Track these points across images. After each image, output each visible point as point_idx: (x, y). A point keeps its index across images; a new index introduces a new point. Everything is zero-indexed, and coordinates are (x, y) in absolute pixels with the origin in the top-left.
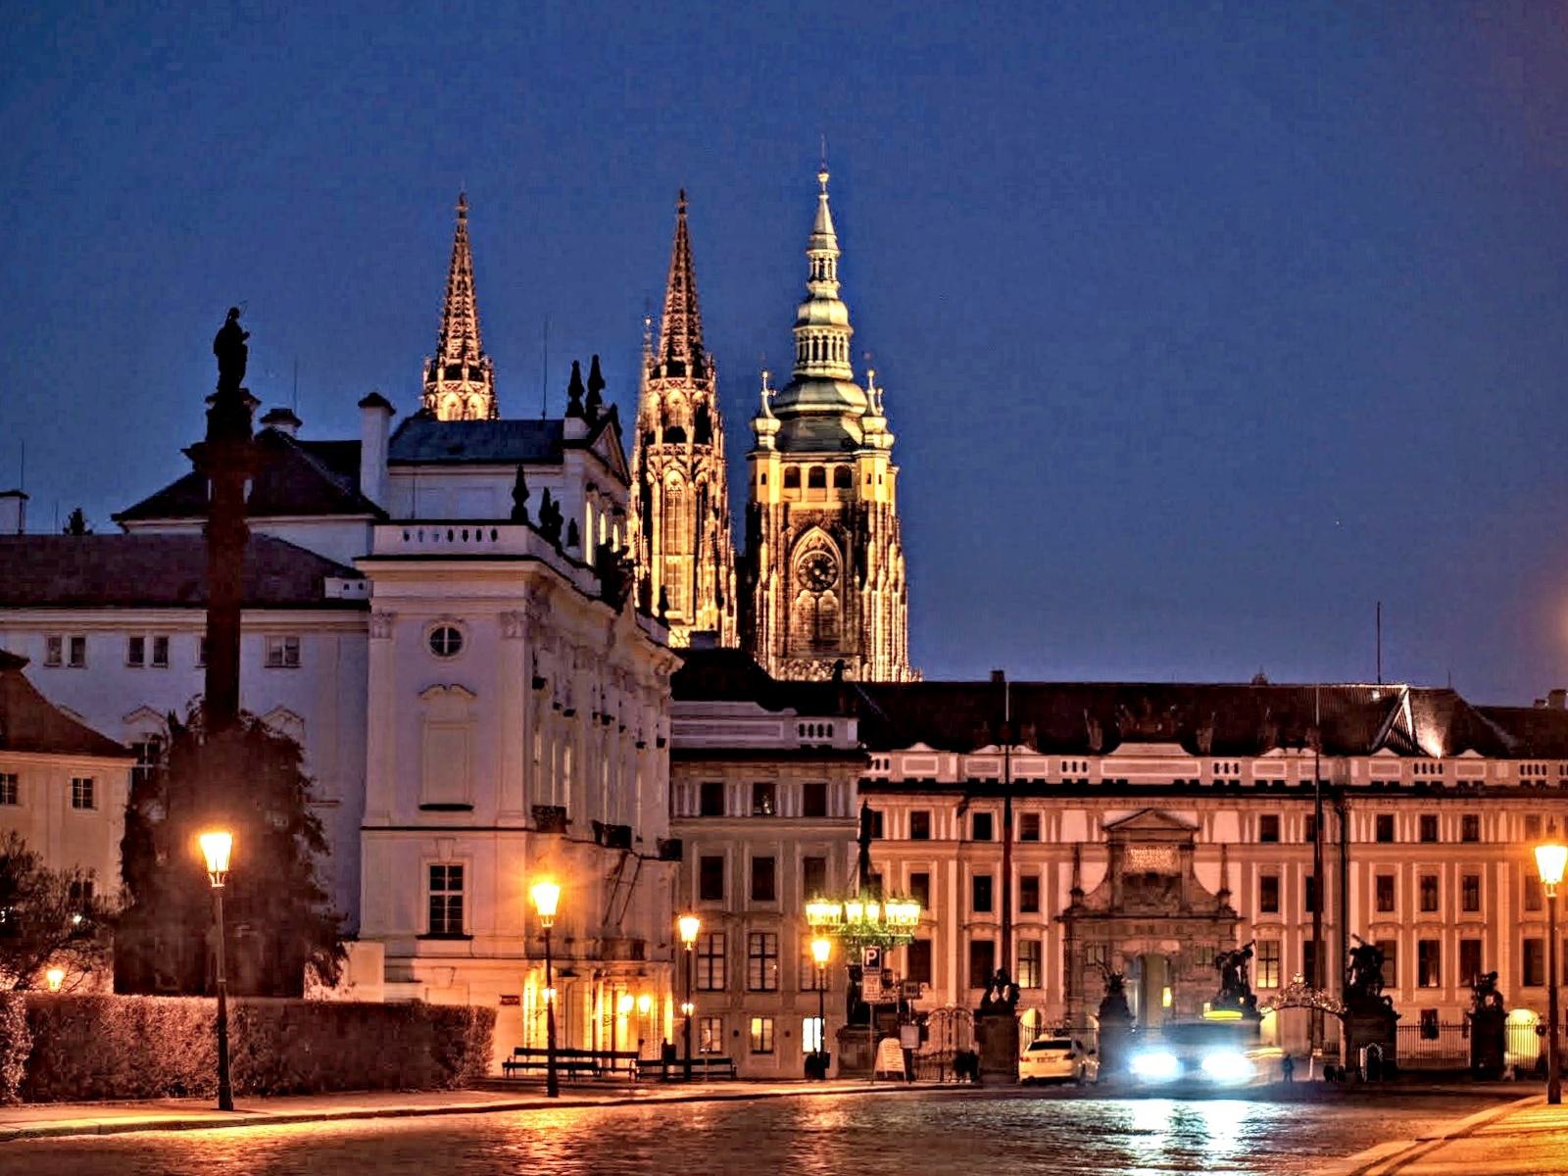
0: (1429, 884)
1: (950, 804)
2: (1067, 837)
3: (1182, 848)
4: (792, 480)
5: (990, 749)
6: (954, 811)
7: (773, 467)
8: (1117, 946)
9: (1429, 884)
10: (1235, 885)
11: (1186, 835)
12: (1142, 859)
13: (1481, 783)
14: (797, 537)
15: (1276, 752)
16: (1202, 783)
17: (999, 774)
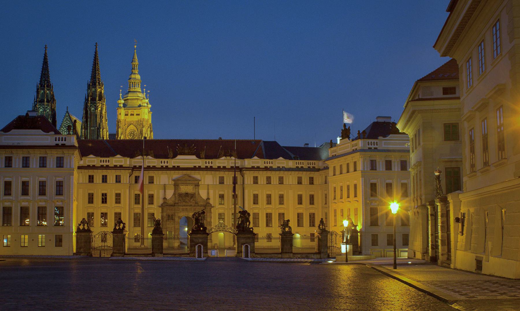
0: (269, 197)
1: (127, 173)
2: (162, 183)
3: (195, 186)
4: (126, 115)
5: (140, 157)
6: (128, 175)
7: (122, 111)
8: (176, 214)
9: (269, 197)
10: (211, 197)
11: (196, 182)
12: (184, 189)
13: (284, 167)
14: (127, 127)
15: (224, 158)
16: (202, 167)
17: (142, 164)
